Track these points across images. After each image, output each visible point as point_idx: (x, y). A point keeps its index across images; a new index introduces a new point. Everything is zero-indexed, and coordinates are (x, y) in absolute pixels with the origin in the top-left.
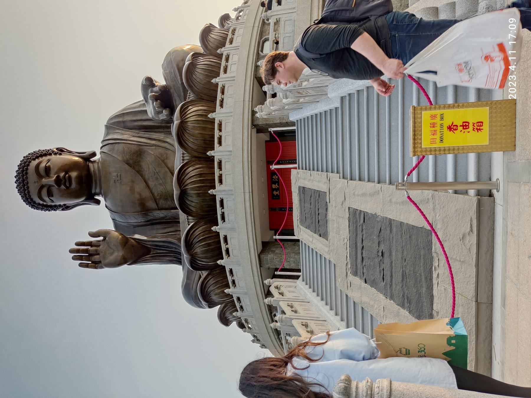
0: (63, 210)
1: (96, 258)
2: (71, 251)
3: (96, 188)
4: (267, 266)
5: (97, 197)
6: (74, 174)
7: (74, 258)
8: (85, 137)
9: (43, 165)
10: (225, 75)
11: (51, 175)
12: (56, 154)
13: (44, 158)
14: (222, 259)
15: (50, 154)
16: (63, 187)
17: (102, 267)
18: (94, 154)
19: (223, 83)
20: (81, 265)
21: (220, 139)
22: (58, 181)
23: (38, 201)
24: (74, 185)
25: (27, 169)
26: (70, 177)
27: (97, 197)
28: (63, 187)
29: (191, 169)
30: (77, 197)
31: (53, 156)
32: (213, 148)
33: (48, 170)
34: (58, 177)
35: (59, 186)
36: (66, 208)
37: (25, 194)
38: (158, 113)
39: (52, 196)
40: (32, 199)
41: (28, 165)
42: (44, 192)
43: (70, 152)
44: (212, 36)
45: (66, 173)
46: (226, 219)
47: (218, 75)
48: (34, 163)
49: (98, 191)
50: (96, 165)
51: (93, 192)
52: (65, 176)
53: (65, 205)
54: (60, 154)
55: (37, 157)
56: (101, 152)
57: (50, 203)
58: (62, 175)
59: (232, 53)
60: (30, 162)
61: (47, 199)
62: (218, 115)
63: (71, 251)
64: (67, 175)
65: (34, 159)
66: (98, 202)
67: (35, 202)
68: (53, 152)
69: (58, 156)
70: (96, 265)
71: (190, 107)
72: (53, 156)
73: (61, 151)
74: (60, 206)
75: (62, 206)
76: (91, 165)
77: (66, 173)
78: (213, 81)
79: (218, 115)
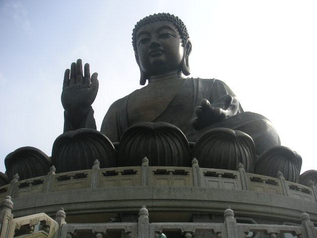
0: (136, 55)
2: (79, 61)
3: (154, 78)
5: (147, 81)
6: (163, 58)
7: (73, 65)
9: (170, 32)
10: (202, 174)
11: (160, 40)
12: (183, 42)
13: (178, 33)
15: (182, 37)
16: (150, 50)
18: (187, 73)
19: (191, 174)
20: (67, 71)
21: (114, 174)
22: (155, 46)
23: (138, 33)
24: (152, 60)
25: (164, 20)
26: (159, 55)
27: (147, 81)
31: (181, 40)
33: (166, 36)
34: (158, 45)
39: (143, 43)
41: (169, 21)
42: (144, 37)
44: (290, 165)
45: (163, 51)
46: (22, 190)
47: (202, 165)
48: (171, 25)
49: (152, 80)
50: (177, 75)
51: (152, 77)
54: (183, 46)
55: (177, 27)
56: (189, 79)
57: (138, 43)
58: (162, 48)
59: (237, 182)
60: (172, 22)
63: (79, 61)
64: (161, 52)
65: (175, 25)
66: (142, 82)
68: (186, 40)
69: (181, 44)
70: (67, 82)
73: (188, 47)
76: (177, 71)
77: (163, 51)
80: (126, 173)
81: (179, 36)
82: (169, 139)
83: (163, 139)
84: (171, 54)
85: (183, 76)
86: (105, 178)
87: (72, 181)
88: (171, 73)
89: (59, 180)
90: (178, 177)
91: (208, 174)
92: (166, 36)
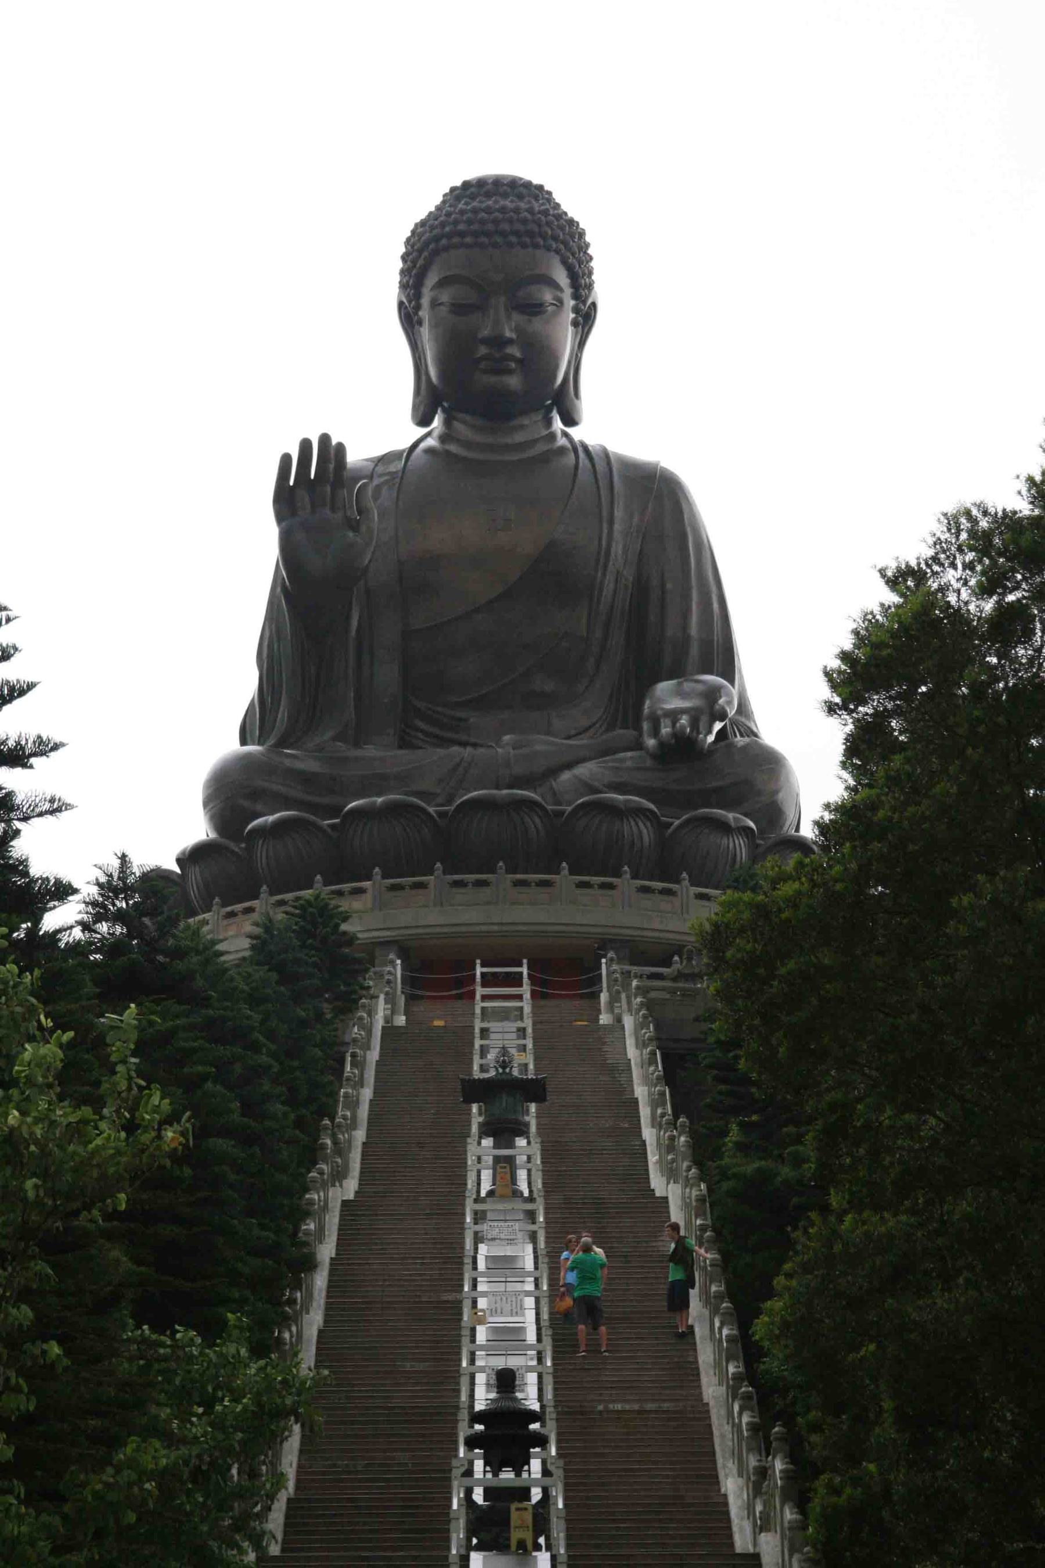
0: (401, 304)
1: (304, 498)
2: (325, 439)
4: (377, 954)
6: (514, 382)
7: (305, 446)
9: (548, 296)
12: (576, 310)
14: (384, 877)
15: (576, 296)
17: (280, 518)
18: (570, 420)
20: (286, 459)
29: (537, 820)
30: (443, 373)
31: (572, 303)
32: (572, 872)
35: (485, 341)
36: (409, 319)
37: (462, 234)
40: (446, 249)
41: (548, 249)
46: (454, 890)
52: (512, 358)
53: (420, 323)
54: (575, 324)
58: (515, 351)
61: (445, 297)
62: (626, 883)
64: (513, 365)
66: (423, 419)
67: (436, 253)
71: (648, 824)
72: (572, 303)
73: (585, 319)
74: (418, 307)
75: (416, 314)
78: (684, 875)
79: (626, 883)
80: (603, 886)
81: (568, 292)
82: (640, 824)
83: (633, 823)
84: (538, 359)
85: (558, 424)
86: (579, 891)
89: (515, 885)
90: (666, 898)
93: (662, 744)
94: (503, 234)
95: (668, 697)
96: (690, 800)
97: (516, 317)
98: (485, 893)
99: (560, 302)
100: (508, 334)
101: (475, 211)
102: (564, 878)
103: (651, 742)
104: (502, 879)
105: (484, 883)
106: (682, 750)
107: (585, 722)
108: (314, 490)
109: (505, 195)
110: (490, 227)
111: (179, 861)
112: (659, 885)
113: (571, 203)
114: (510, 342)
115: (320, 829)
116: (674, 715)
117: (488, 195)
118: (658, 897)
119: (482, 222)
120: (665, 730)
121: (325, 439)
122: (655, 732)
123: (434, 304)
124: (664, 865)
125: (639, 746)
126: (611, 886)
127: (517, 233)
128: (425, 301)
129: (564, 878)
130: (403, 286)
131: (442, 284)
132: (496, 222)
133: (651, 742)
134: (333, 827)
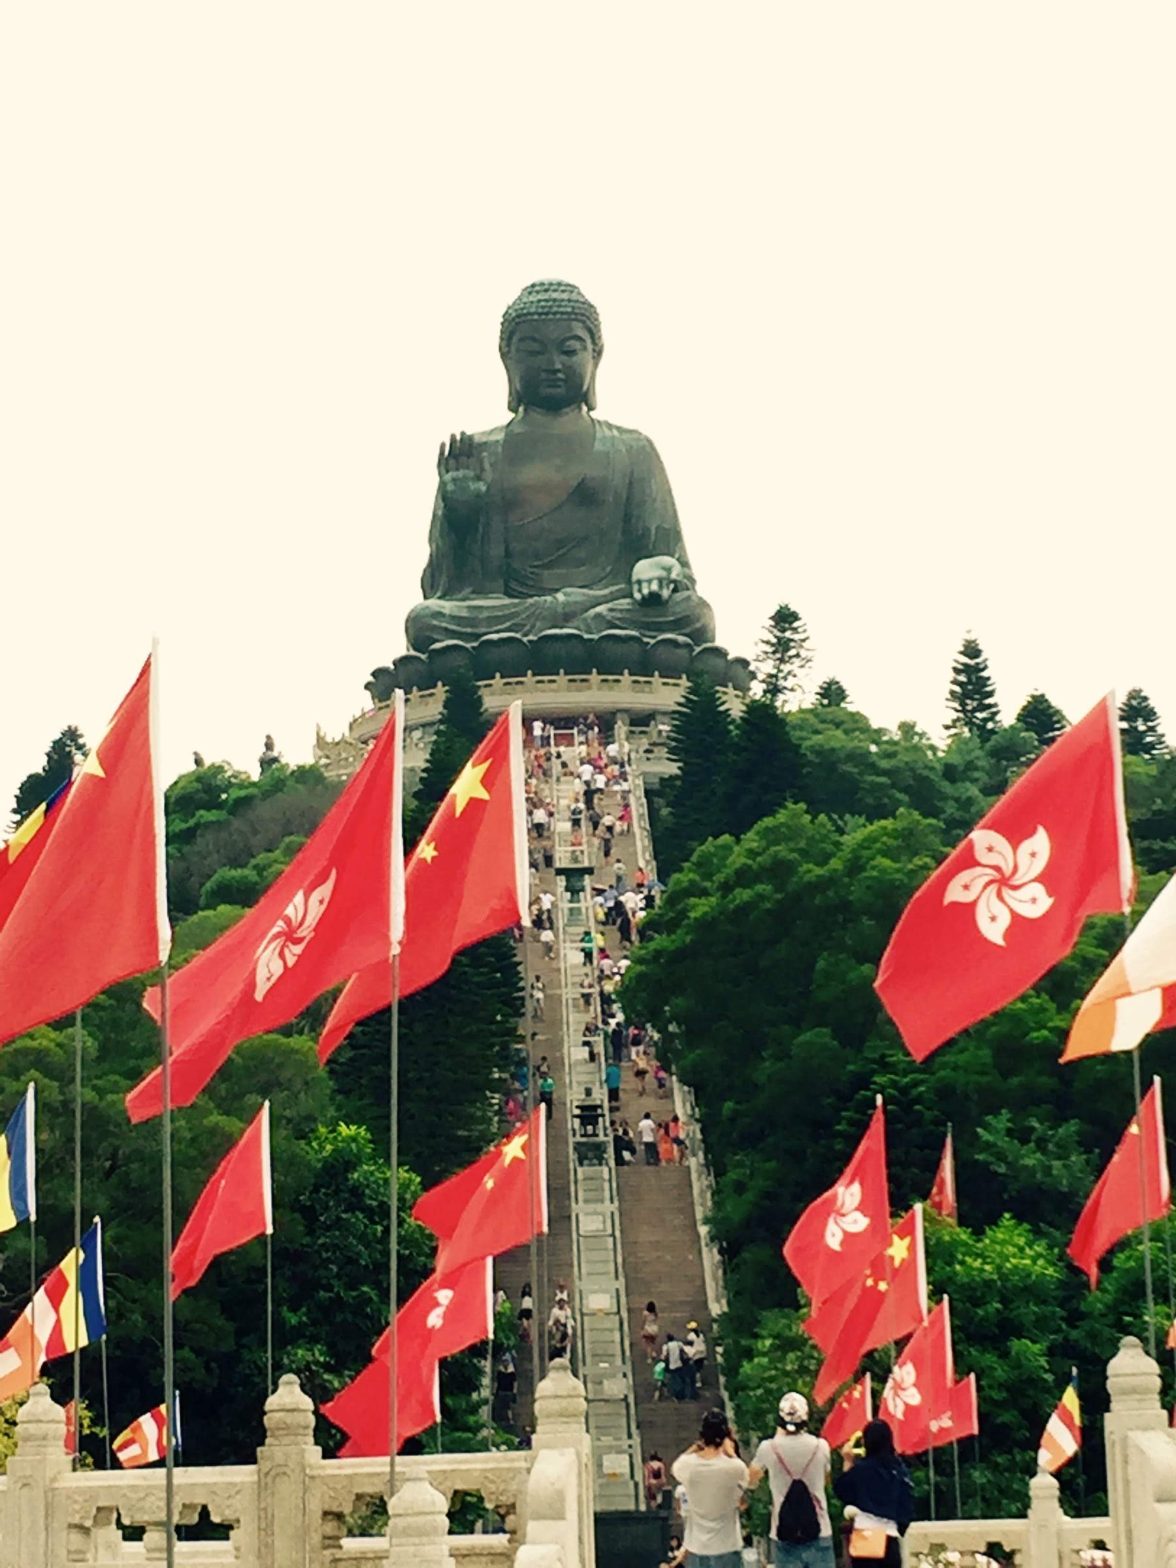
2: (463, 434)
7: (453, 437)
8: (620, 396)
15: (594, 343)
18: (591, 408)
20: (443, 446)
28: (544, 375)
30: (523, 387)
32: (599, 673)
33: (571, 353)
36: (504, 356)
38: (639, 582)
42: (535, 346)
43: (596, 365)
58: (560, 375)
62: (626, 678)
66: (512, 408)
73: (598, 353)
81: (589, 341)
85: (585, 408)
87: (578, 683)
88: (566, 410)
91: (664, 684)
92: (571, 353)
93: (643, 597)
94: (555, 314)
95: (646, 570)
96: (660, 628)
97: (564, 358)
98: (554, 686)
99: (585, 348)
100: (558, 366)
101: (539, 301)
102: (594, 677)
103: (638, 596)
104: (562, 679)
105: (554, 681)
106: (653, 600)
107: (603, 575)
108: (459, 454)
109: (555, 291)
110: (546, 310)
111: (394, 663)
112: (642, 679)
113: (591, 293)
114: (559, 371)
115: (466, 649)
116: (650, 581)
117: (546, 291)
118: (643, 685)
119: (543, 307)
120: (646, 591)
121: (463, 434)
122: (640, 591)
123: (518, 350)
124: (645, 665)
125: (631, 596)
126: (618, 681)
127: (562, 313)
128: (513, 348)
129: (594, 677)
130: (502, 339)
131: (521, 340)
132: (551, 307)
133: (638, 596)
134: (473, 648)
